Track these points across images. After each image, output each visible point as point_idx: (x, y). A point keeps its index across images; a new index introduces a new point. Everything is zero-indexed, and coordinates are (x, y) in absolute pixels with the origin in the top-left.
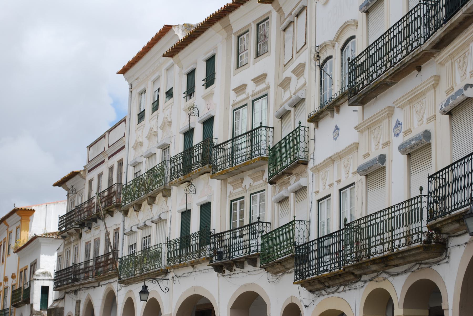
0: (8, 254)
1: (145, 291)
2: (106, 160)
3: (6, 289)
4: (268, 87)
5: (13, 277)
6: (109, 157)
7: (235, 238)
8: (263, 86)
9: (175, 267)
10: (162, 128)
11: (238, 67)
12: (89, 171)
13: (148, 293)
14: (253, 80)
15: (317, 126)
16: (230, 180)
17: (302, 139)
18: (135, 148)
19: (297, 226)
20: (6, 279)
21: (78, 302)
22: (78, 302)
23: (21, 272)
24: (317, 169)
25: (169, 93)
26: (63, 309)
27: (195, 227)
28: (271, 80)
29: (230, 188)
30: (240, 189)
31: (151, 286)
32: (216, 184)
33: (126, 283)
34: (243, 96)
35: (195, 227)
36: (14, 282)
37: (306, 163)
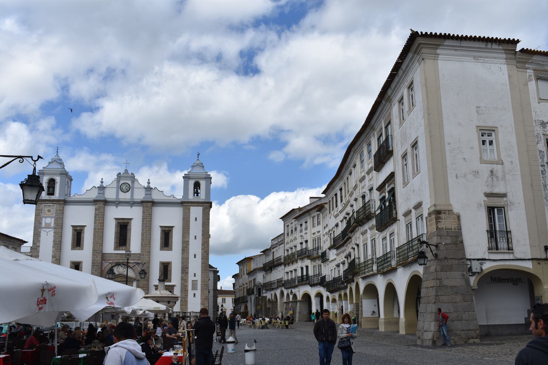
0: (244, 275)
1: (291, 292)
2: (278, 246)
3: (244, 288)
4: (321, 235)
5: (246, 284)
6: (279, 245)
7: (315, 277)
8: (319, 234)
9: (301, 285)
10: (294, 240)
11: (313, 227)
12: (272, 249)
13: (293, 293)
14: (317, 232)
15: (330, 251)
16: (313, 260)
17: (327, 253)
19: (326, 276)
20: (243, 285)
21: (272, 294)
22: (272, 294)
23: (250, 282)
24: (330, 262)
25: (296, 229)
26: (266, 296)
27: (305, 273)
28: (321, 232)
29: (313, 262)
30: (315, 263)
31: (293, 290)
32: (309, 261)
33: (287, 288)
34: (315, 236)
35: (305, 273)
36: (247, 286)
37: (328, 260)
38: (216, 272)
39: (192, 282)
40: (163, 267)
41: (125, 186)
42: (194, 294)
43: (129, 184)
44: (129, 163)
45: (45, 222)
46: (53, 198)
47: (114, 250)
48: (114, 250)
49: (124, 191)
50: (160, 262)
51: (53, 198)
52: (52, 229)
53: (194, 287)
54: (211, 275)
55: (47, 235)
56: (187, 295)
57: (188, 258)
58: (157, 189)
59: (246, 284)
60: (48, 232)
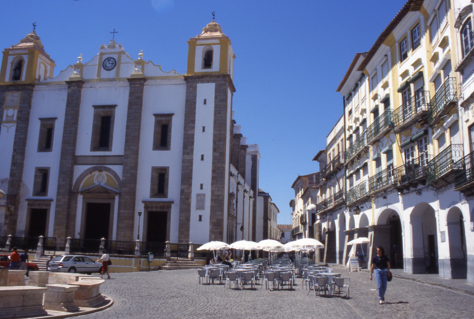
5: (301, 210)
18: (348, 130)
38: (266, 197)
39: (197, 197)
40: (156, 175)
41: (108, 63)
42: (200, 217)
43: (114, 59)
44: (117, 32)
45: (7, 115)
46: (18, 82)
47: (91, 151)
48: (91, 151)
49: (108, 69)
50: (153, 167)
51: (18, 82)
52: (14, 124)
53: (200, 207)
54: (260, 200)
55: (8, 131)
56: (188, 219)
57: (191, 162)
58: (153, 63)
59: (301, 210)
60: (10, 127)
